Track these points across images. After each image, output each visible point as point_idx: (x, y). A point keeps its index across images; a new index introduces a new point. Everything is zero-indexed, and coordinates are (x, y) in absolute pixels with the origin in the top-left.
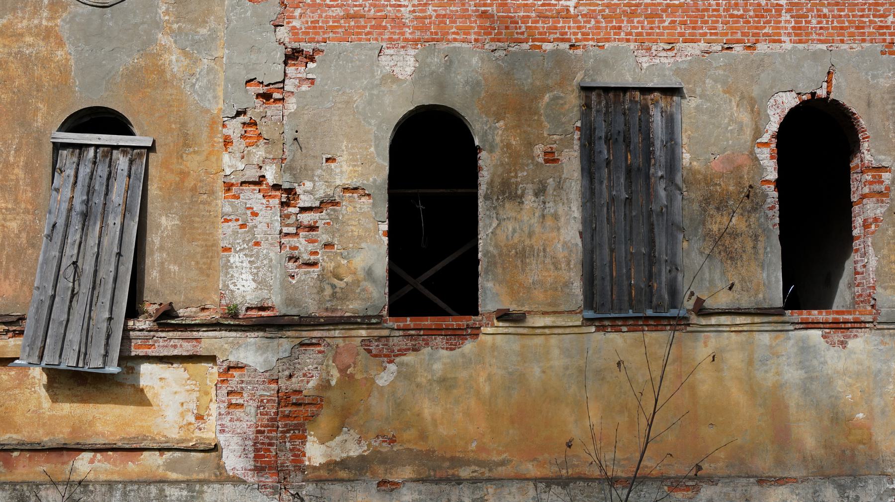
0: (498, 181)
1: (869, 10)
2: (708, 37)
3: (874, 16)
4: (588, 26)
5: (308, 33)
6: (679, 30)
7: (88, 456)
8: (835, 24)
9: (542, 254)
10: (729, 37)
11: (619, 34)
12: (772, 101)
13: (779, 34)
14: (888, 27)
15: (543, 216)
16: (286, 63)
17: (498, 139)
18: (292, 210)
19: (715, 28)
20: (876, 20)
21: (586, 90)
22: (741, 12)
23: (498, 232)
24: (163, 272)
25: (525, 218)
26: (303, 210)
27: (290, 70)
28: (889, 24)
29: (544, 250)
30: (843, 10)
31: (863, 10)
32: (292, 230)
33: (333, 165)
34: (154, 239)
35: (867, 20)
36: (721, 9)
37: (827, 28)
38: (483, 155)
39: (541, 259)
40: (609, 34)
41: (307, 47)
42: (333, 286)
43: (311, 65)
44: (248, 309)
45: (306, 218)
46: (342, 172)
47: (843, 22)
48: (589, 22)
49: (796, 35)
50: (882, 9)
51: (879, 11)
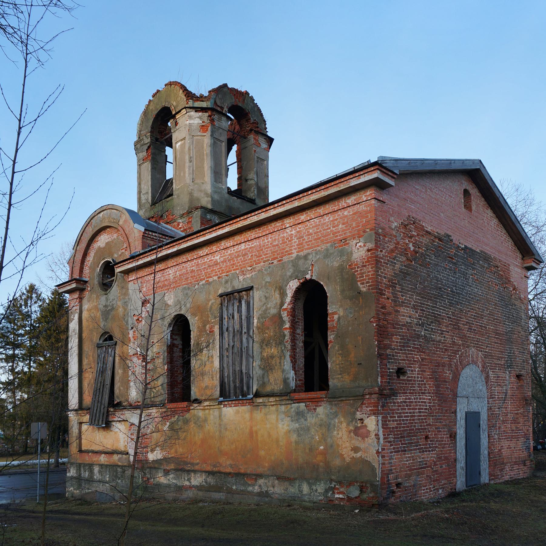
0: (196, 343)
1: (330, 224)
2: (265, 259)
4: (223, 266)
6: (254, 259)
7: (103, 455)
8: (315, 237)
10: (272, 257)
11: (233, 267)
12: (288, 286)
13: (291, 250)
14: (339, 232)
15: (209, 357)
16: (142, 306)
19: (266, 254)
20: (334, 229)
21: (221, 296)
22: (277, 243)
23: (196, 366)
24: (120, 390)
25: (203, 359)
31: (328, 225)
34: (117, 378)
35: (329, 230)
36: (269, 243)
38: (192, 332)
39: (208, 376)
40: (230, 268)
42: (154, 392)
44: (135, 402)
47: (319, 235)
48: (223, 265)
49: (299, 248)
50: (336, 222)
51: (335, 223)
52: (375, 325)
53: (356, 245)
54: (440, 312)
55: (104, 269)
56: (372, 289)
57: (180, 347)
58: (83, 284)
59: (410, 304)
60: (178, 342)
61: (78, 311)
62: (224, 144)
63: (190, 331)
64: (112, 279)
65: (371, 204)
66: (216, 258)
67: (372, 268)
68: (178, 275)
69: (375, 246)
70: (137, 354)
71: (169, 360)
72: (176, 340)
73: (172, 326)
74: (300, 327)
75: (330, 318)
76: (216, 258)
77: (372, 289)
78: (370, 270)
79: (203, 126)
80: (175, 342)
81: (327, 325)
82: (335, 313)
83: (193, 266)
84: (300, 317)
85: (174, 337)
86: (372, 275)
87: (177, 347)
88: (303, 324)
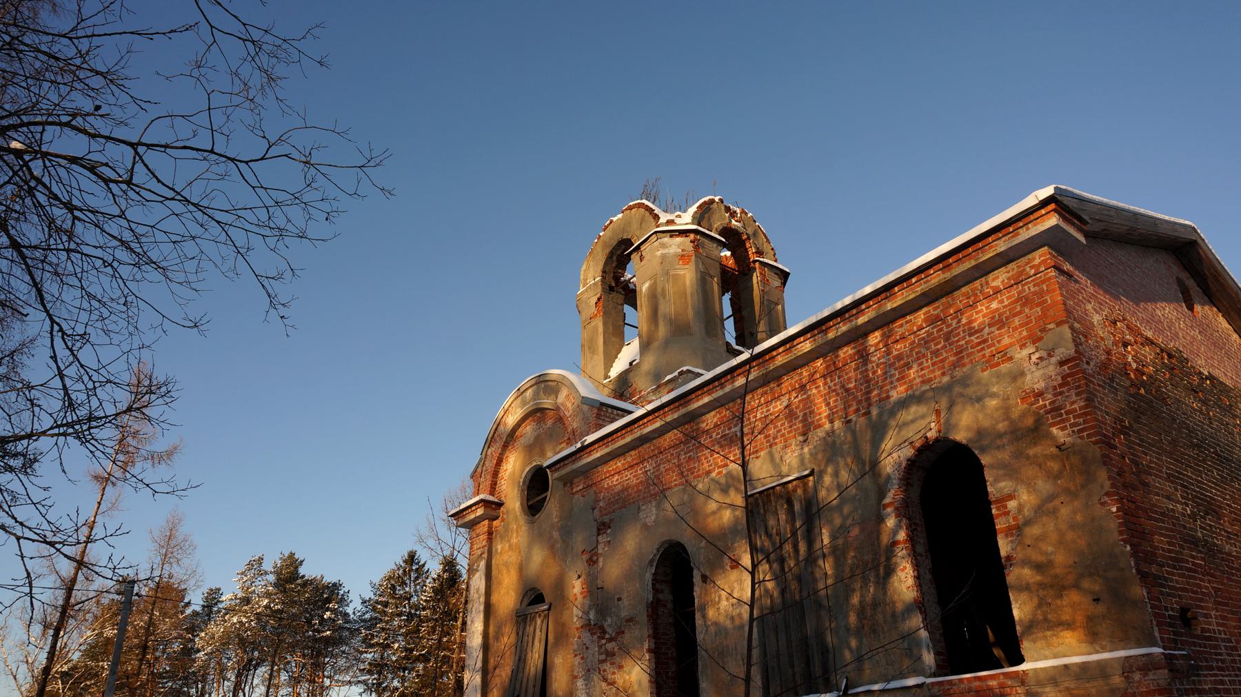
3: (970, 335)
5: (605, 509)
9: (734, 652)
17: (702, 557)
18: (603, 641)
20: (973, 338)
26: (610, 640)
27: (600, 538)
28: (986, 337)
29: (736, 649)
30: (940, 343)
32: (603, 657)
33: (620, 603)
35: (963, 342)
37: (928, 367)
41: (606, 519)
43: (609, 531)
45: (609, 646)
46: (624, 607)
52: (1114, 509)
53: (1030, 358)
54: (1211, 493)
55: (531, 480)
56: (1089, 436)
57: (670, 605)
58: (495, 509)
59: (1161, 471)
60: (666, 596)
61: (485, 556)
62: (715, 279)
63: (692, 570)
64: (543, 496)
65: (1049, 279)
66: (733, 430)
67: (1077, 395)
68: (664, 470)
69: (1076, 352)
70: (590, 625)
71: (651, 631)
72: (662, 592)
73: (655, 564)
74: (922, 541)
75: (998, 509)
76: (733, 430)
77: (1089, 436)
78: (1074, 398)
79: (683, 256)
80: (661, 596)
81: (993, 525)
82: (1011, 497)
83: (690, 451)
84: (917, 521)
85: (658, 586)
86: (1081, 408)
87: (665, 606)
88: (925, 535)
